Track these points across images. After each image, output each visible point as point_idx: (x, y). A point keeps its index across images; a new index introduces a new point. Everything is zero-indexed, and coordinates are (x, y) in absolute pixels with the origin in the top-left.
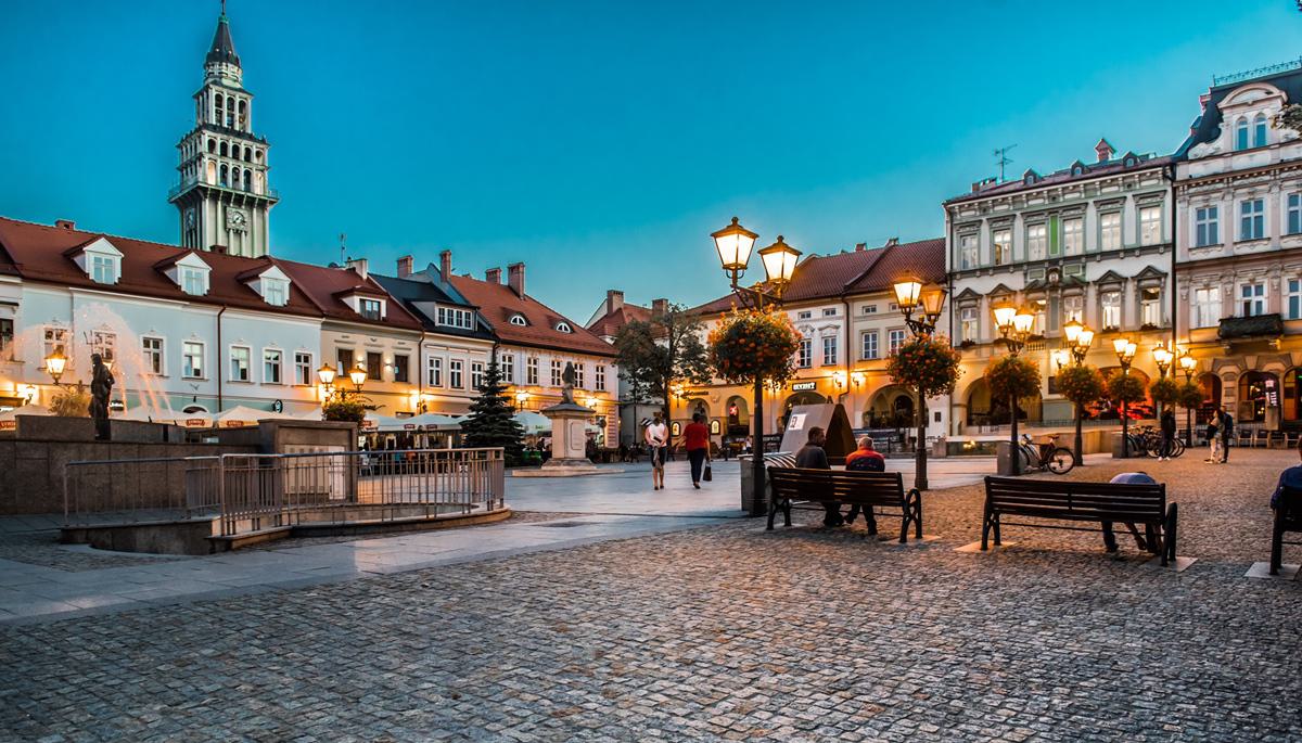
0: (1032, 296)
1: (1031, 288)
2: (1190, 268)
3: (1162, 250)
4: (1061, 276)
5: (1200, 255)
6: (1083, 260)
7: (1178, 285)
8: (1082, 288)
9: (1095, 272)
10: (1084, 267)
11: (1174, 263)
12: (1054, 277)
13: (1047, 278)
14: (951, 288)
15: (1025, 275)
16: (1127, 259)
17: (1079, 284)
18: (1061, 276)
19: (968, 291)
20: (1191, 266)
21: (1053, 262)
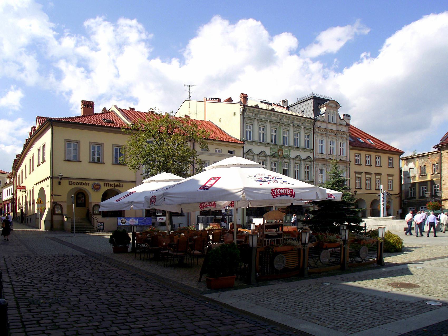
0: (274, 159)
1: (273, 156)
2: (319, 160)
3: (311, 151)
4: (283, 153)
5: (320, 156)
6: (290, 148)
7: (315, 165)
8: (290, 160)
9: (293, 154)
10: (290, 151)
11: (314, 158)
12: (280, 153)
13: (278, 153)
14: (243, 148)
15: (271, 149)
16: (306, 152)
17: (288, 158)
18: (283, 153)
19: (250, 150)
20: (319, 159)
21: (281, 146)
